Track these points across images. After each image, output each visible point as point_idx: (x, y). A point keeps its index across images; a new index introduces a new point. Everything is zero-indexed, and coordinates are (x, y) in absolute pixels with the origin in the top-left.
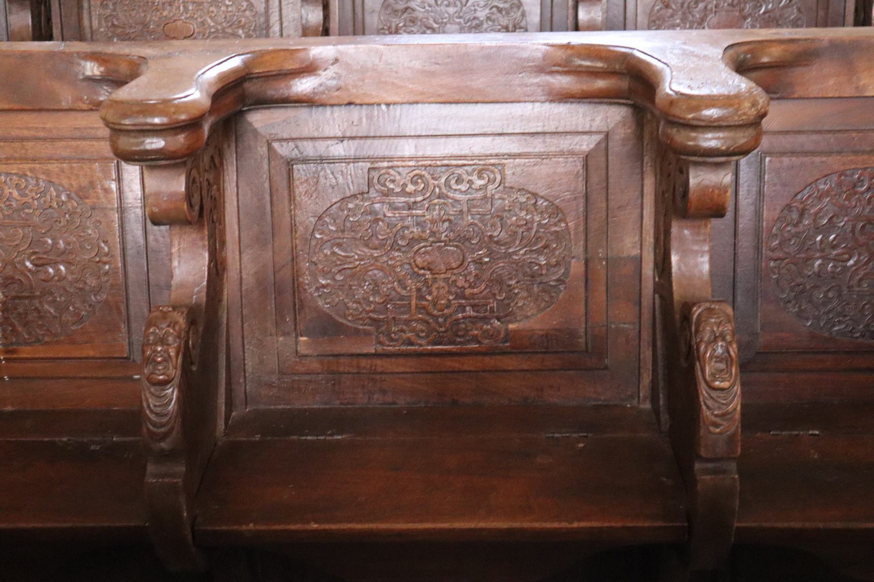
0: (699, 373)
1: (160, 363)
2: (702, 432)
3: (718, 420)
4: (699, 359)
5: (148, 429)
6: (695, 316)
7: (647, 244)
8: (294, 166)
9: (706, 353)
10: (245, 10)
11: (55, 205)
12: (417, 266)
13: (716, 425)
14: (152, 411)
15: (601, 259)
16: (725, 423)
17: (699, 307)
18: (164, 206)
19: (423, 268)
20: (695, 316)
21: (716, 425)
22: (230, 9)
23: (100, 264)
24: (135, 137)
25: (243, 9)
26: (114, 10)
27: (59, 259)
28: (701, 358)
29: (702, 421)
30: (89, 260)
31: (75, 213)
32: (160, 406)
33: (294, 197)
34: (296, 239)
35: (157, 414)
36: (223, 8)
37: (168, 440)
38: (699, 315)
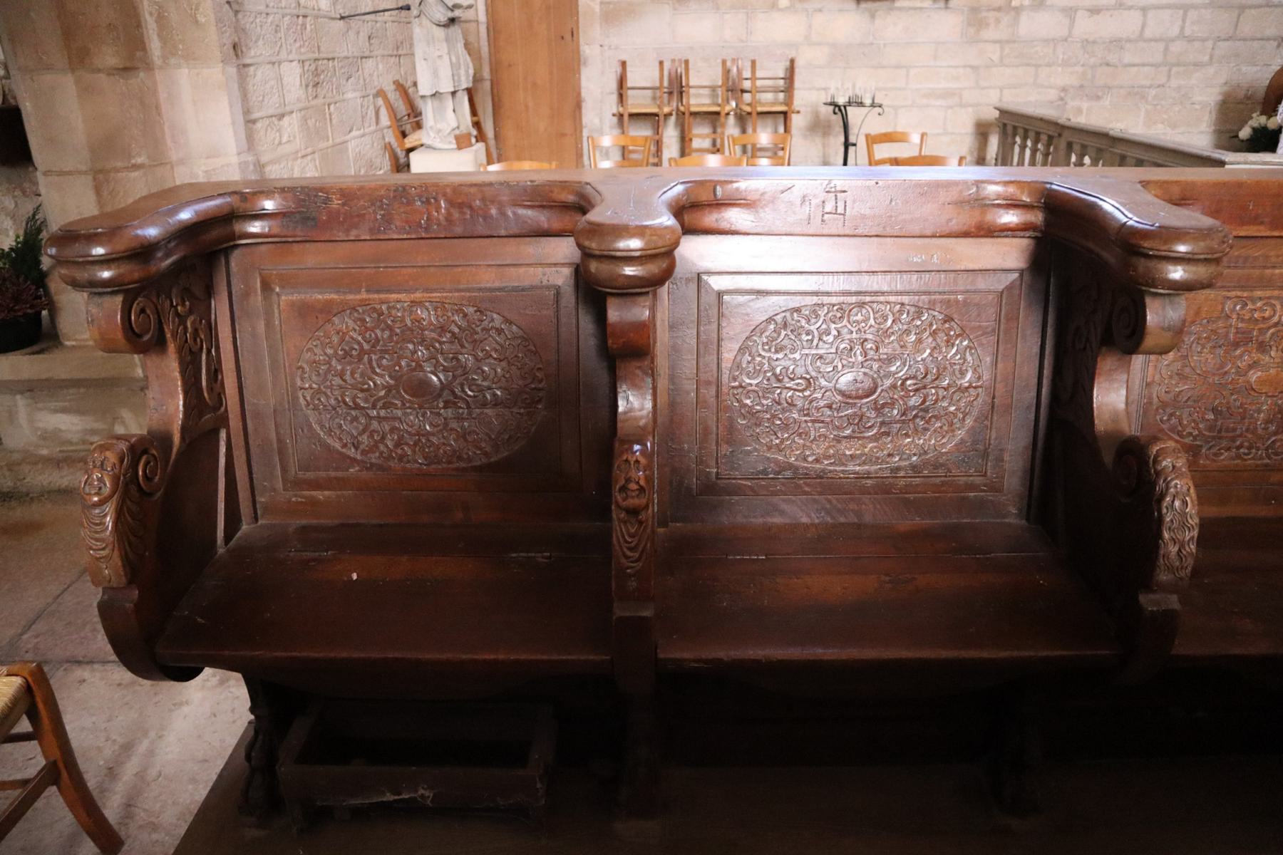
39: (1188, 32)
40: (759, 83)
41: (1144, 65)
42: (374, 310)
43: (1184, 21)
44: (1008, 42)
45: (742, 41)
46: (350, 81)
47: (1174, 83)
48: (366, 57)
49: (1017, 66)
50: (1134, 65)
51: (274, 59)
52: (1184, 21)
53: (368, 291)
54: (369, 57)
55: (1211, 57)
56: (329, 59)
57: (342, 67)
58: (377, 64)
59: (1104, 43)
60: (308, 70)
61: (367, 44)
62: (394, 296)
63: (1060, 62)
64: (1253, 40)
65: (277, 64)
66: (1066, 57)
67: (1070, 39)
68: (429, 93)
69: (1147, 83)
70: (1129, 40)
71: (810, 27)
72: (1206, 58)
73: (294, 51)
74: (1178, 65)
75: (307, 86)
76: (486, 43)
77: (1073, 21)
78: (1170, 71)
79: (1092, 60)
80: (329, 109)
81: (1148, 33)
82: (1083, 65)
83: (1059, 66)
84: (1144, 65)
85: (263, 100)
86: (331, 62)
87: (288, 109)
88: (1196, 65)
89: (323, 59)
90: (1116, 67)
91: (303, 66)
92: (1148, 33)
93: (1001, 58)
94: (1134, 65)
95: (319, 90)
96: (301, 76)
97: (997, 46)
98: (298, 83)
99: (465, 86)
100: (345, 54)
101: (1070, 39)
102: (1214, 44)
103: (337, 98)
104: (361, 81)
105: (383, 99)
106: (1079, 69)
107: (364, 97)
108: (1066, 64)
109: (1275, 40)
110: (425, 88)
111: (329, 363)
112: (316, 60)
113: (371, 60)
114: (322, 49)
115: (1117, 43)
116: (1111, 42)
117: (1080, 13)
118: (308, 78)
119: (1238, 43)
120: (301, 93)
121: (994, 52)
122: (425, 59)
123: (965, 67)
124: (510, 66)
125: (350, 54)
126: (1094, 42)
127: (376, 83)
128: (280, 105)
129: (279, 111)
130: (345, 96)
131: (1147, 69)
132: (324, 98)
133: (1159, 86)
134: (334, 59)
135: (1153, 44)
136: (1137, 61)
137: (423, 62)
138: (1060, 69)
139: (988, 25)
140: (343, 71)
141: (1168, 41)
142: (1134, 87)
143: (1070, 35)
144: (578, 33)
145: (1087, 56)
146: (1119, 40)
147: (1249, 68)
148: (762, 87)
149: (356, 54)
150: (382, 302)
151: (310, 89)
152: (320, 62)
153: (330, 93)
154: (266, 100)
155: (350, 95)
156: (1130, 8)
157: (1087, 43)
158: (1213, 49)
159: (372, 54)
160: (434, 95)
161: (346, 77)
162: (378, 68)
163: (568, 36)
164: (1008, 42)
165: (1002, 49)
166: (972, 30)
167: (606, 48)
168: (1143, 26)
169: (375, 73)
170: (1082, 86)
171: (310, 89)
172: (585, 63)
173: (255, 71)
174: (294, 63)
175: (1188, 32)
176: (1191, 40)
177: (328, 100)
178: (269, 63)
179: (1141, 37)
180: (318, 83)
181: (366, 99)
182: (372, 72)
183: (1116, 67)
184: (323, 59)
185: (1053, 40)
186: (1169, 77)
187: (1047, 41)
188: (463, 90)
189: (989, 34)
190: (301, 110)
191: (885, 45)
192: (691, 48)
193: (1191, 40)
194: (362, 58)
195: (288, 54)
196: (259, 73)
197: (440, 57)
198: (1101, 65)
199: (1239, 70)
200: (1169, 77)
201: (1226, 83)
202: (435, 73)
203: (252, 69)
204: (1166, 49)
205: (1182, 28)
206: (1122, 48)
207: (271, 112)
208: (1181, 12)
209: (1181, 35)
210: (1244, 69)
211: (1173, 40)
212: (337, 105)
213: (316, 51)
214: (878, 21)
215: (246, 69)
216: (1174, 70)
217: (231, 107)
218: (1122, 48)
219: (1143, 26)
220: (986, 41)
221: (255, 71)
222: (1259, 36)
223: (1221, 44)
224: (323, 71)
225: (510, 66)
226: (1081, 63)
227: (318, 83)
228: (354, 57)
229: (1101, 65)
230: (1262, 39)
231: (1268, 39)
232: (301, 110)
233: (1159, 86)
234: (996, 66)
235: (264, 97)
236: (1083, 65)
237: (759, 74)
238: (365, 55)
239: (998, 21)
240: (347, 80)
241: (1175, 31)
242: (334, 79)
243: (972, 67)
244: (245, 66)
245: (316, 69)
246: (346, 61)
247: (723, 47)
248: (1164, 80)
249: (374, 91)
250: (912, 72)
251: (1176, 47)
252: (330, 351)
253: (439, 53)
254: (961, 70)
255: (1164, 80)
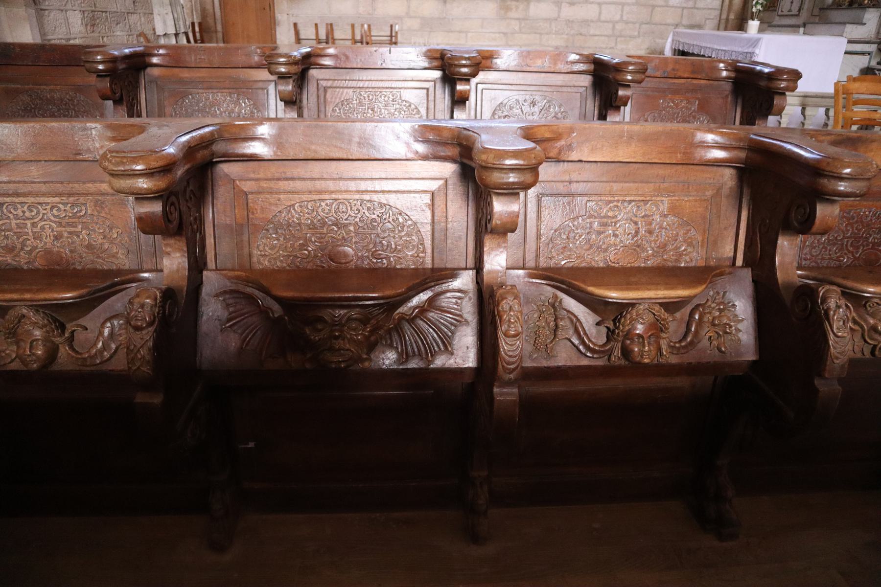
0: (829, 328)
1: (513, 323)
2: (828, 363)
3: (839, 355)
4: (828, 319)
5: (503, 366)
6: (821, 294)
7: (740, 249)
8: (543, 199)
9: (834, 315)
10: (414, 115)
11: (391, 220)
12: (611, 261)
13: (837, 358)
14: (507, 355)
15: (713, 258)
16: (842, 357)
17: (823, 288)
18: (504, 220)
19: (614, 263)
20: (821, 294)
21: (837, 358)
22: (406, 113)
23: (418, 258)
24: (505, 173)
25: (414, 113)
26: (340, 113)
27: (392, 255)
28: (831, 319)
29: (829, 356)
30: (411, 256)
31: (404, 226)
32: (512, 351)
33: (541, 217)
34: (540, 243)
35: (510, 356)
36: (403, 112)
37: (514, 373)
38: (823, 294)
39: (625, 18)
40: (373, 38)
41: (601, 36)
42: (35, 92)
43: (622, 11)
44: (524, 19)
45: (369, 14)
46: (119, 26)
47: (619, 46)
48: (131, 13)
49: (529, 34)
50: (596, 36)
51: (62, 8)
52: (622, 11)
53: (33, 85)
54: (134, 13)
55: (639, 33)
56: (102, 12)
57: (112, 17)
58: (140, 18)
59: (578, 22)
60: (87, 17)
61: (132, 6)
62: (42, 87)
63: (554, 32)
64: (661, 24)
65: (64, 12)
66: (557, 29)
67: (559, 19)
68: (162, 34)
69: (604, 46)
70: (592, 21)
71: (409, 7)
72: (636, 33)
73: (77, 5)
74: (621, 36)
75: (86, 25)
76: (219, 11)
77: (560, 8)
78: (616, 39)
79: (572, 32)
80: (103, 39)
81: (603, 18)
82: (567, 34)
83: (554, 34)
84: (601, 36)
85: (55, 30)
86: (104, 14)
87: (72, 36)
88: (630, 37)
89: (98, 11)
90: (585, 35)
91: (84, 14)
92: (603, 18)
93: (520, 30)
94: (596, 36)
95: (95, 28)
96: (82, 20)
97: (517, 22)
98: (80, 22)
99: (183, 30)
100: (115, 10)
101: (559, 19)
102: (640, 25)
103: (109, 34)
104: (128, 27)
105: (144, 38)
106: (566, 37)
107: (129, 35)
108: (557, 33)
109: (672, 25)
110: (160, 31)
111: (19, 112)
112: (92, 11)
113: (135, 15)
114: (97, 5)
115: (586, 22)
116: (582, 22)
117: (563, 4)
118: (87, 21)
119: (653, 26)
120: (82, 29)
121: (515, 25)
122: (159, 15)
123: (499, 33)
124: (233, 24)
125: (119, 10)
126: (573, 21)
127: (139, 29)
128: (67, 33)
129: (64, 37)
130: (115, 34)
131: (603, 38)
132: (99, 33)
133: (610, 48)
134: (107, 12)
135: (606, 24)
136: (597, 33)
137: (158, 17)
138: (554, 36)
139: (511, 9)
140: (113, 19)
141: (614, 23)
142: (596, 48)
143: (559, 17)
144: (274, 6)
145: (569, 29)
146: (587, 21)
147: (660, 40)
148: (375, 40)
149: (123, 10)
150: (38, 89)
151: (89, 28)
152: (96, 13)
153: (104, 31)
154: (57, 30)
155: (118, 33)
156: (592, 3)
157: (569, 22)
158: (639, 28)
159: (135, 12)
160: (165, 35)
161: (116, 22)
162: (140, 21)
163: (267, 8)
164: (524, 19)
165: (520, 24)
166: (503, 12)
167: (291, 16)
168: (600, 13)
169: (139, 23)
170: (567, 47)
171: (89, 28)
172: (278, 25)
173: (49, 13)
174: (76, 12)
175: (625, 18)
176: (627, 23)
177: (103, 35)
178: (59, 10)
179: (599, 20)
180: (95, 24)
181: (131, 37)
182: (136, 22)
183: (585, 35)
184: (98, 11)
185: (549, 19)
186: (616, 43)
187: (546, 20)
188: (183, 33)
189: (513, 14)
190: (82, 38)
191: (452, 19)
192: (340, 17)
193: (627, 23)
194: (128, 13)
195: (72, 6)
196: (52, 15)
197: (167, 14)
198: (577, 35)
199: (655, 41)
200: (616, 43)
201: (648, 49)
202: (165, 22)
203: (47, 12)
204: (614, 27)
205: (622, 16)
206: (589, 25)
207: (60, 37)
208: (620, 7)
209: (621, 20)
210: (658, 41)
211: (617, 22)
212: (109, 38)
213: (93, 5)
214: (448, 5)
215: (43, 12)
216: (619, 39)
217: (32, 31)
218: (589, 25)
219: (600, 13)
220: (511, 19)
221: (49, 13)
222: (664, 23)
223: (644, 26)
224: (98, 18)
225: (233, 24)
226: (566, 33)
227: (95, 24)
228: (122, 12)
229: (577, 35)
230: (665, 25)
231: (669, 25)
232: (82, 38)
233: (610, 48)
234: (518, 33)
235: (55, 28)
236: (567, 34)
237: (372, 34)
238: (131, 11)
239: (517, 7)
240: (117, 24)
241: (618, 17)
242: (107, 23)
243: (505, 34)
244: (42, 10)
245: (93, 16)
246: (116, 14)
247: (359, 17)
248: (613, 45)
249: (138, 33)
250: (470, 35)
251: (619, 27)
252: (19, 108)
253: (166, 12)
254: (497, 35)
255: (613, 45)
